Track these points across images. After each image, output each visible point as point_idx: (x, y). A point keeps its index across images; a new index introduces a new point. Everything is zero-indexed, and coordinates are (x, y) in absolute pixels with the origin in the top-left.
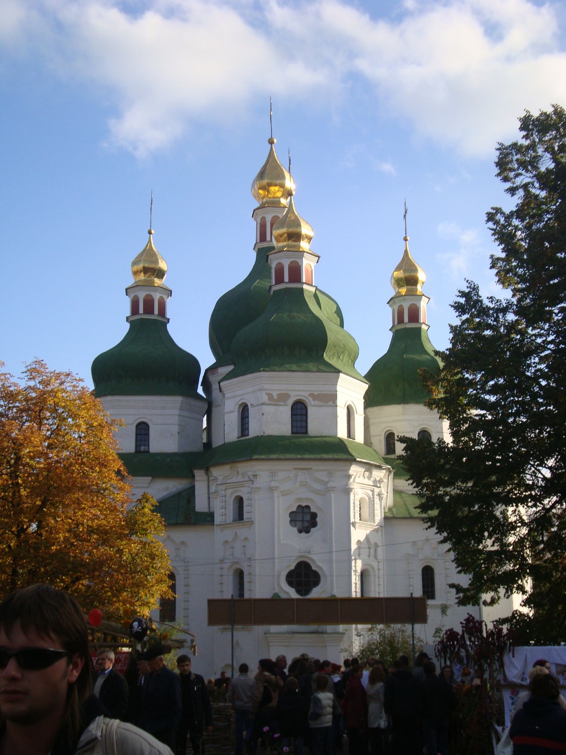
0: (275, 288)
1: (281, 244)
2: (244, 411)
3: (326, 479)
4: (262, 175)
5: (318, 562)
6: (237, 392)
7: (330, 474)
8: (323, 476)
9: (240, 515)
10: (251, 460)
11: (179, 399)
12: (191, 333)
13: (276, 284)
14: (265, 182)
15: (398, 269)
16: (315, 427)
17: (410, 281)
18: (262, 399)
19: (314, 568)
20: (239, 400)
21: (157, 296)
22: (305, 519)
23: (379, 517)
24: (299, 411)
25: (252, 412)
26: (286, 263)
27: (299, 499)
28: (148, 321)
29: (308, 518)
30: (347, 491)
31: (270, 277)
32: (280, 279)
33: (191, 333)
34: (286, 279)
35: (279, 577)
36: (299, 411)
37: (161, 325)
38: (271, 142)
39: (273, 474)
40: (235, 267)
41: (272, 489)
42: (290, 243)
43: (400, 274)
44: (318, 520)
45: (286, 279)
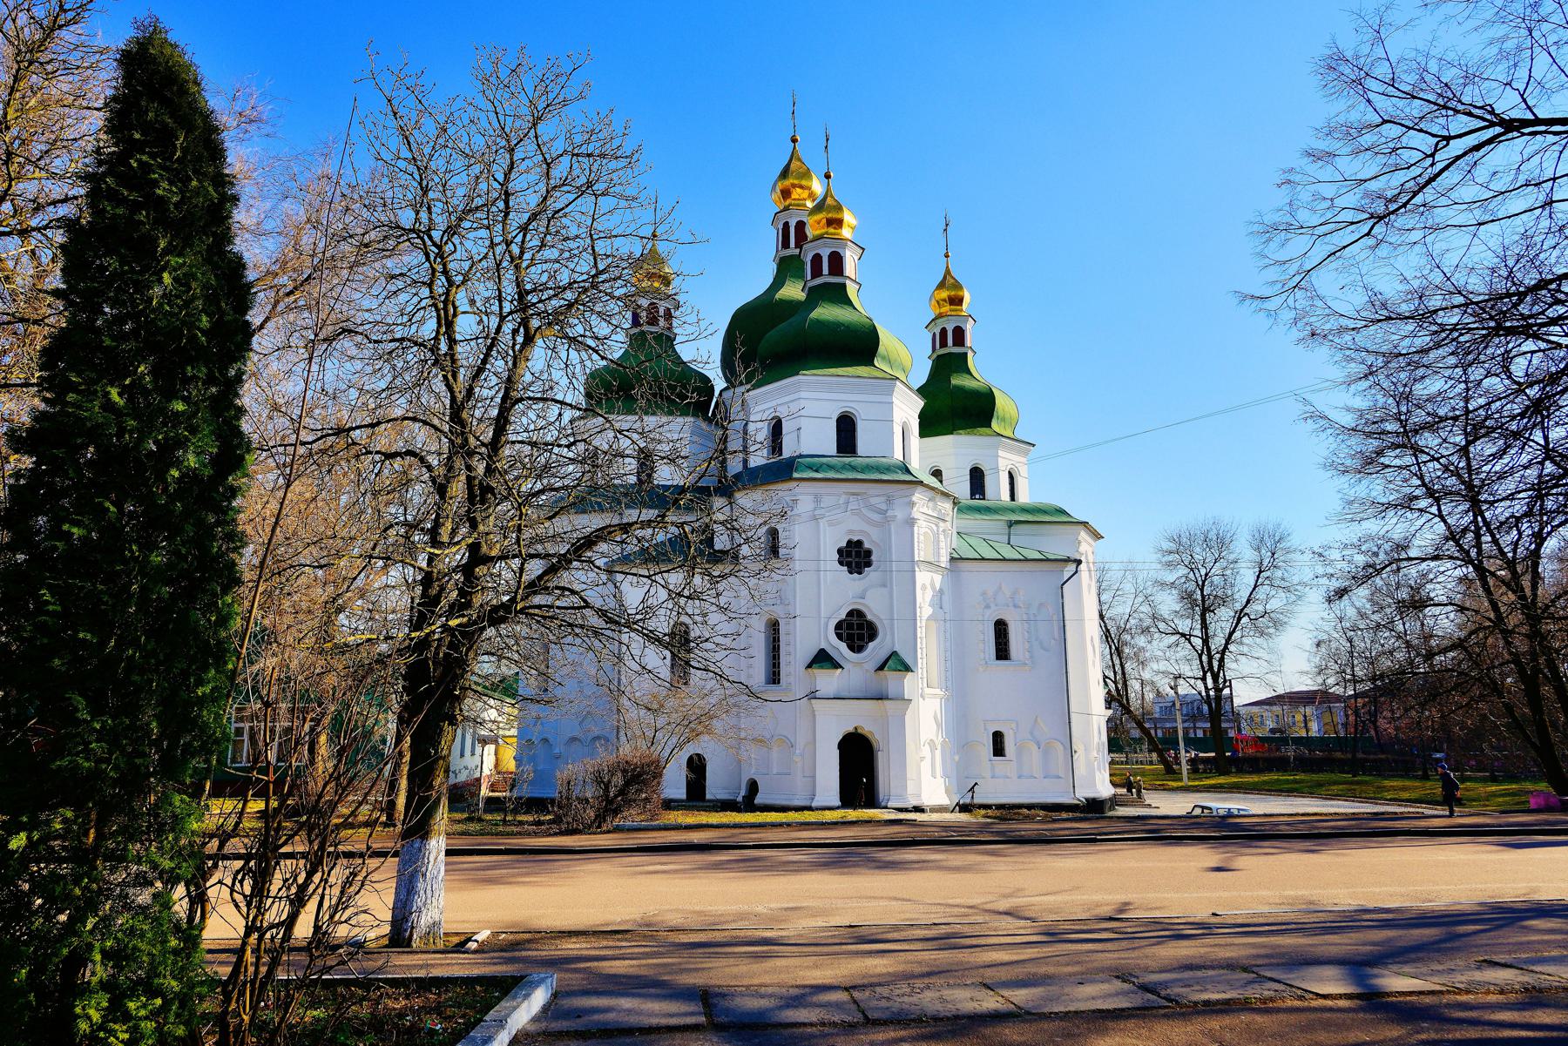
0: (810, 284)
1: (818, 232)
2: (777, 429)
3: (884, 507)
4: (785, 174)
5: (874, 610)
6: (763, 403)
7: (889, 501)
8: (877, 501)
9: (774, 550)
10: (791, 479)
11: (690, 419)
12: (701, 348)
13: (813, 277)
14: (787, 183)
15: (941, 285)
16: (865, 442)
17: (957, 301)
18: (806, 406)
19: (869, 617)
20: (768, 415)
21: (662, 306)
22: (855, 557)
23: (944, 561)
24: (846, 428)
25: (786, 427)
26: (825, 254)
27: (851, 531)
28: (653, 333)
29: (858, 554)
30: (911, 522)
31: (803, 269)
32: (817, 272)
33: (701, 348)
34: (825, 270)
35: (827, 625)
36: (846, 428)
37: (667, 340)
38: (794, 141)
39: (817, 499)
40: (751, 276)
41: (815, 519)
42: (831, 230)
43: (944, 294)
44: (873, 558)
45: (825, 270)
